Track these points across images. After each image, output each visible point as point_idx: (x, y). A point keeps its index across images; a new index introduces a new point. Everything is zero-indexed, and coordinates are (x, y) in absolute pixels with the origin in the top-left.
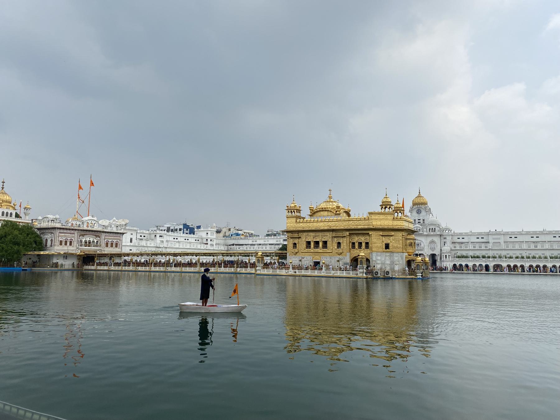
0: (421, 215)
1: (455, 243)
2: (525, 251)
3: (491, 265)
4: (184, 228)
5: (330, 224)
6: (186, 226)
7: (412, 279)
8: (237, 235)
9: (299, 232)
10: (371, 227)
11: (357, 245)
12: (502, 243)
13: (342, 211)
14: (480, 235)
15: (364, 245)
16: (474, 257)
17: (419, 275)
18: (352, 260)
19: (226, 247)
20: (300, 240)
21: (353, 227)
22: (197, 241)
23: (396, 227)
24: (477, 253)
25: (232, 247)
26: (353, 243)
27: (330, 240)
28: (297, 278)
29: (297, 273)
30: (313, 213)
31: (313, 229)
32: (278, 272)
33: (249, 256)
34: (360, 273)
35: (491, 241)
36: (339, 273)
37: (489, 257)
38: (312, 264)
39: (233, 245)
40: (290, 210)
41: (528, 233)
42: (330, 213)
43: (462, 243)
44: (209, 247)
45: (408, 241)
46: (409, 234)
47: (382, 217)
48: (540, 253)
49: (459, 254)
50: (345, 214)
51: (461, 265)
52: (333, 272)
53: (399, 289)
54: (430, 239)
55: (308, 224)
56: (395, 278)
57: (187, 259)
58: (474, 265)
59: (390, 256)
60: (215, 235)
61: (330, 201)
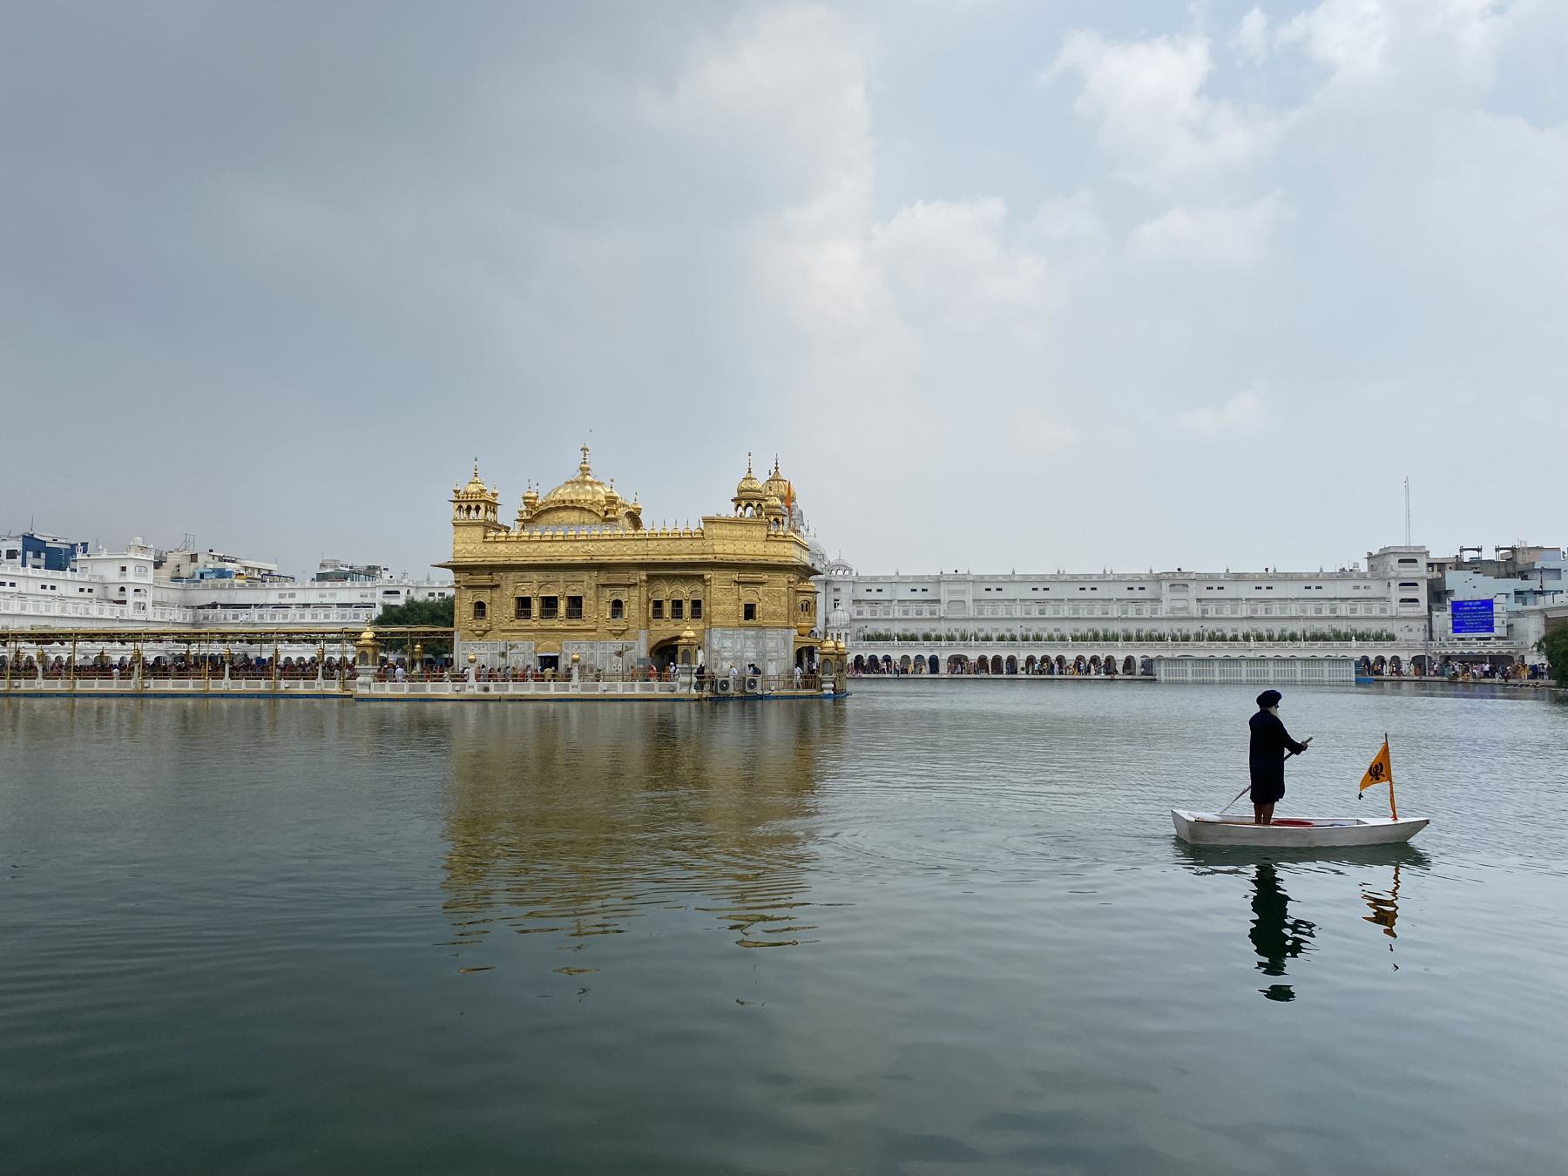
1: (859, 601)
2: (1019, 623)
3: (944, 657)
4: (26, 548)
5: (590, 547)
6: (32, 545)
7: (811, 697)
8: (222, 574)
9: (492, 569)
10: (710, 558)
11: (667, 609)
12: (970, 603)
13: (622, 512)
15: (687, 608)
16: (905, 638)
17: (828, 688)
18: (651, 652)
19: (190, 612)
21: (659, 559)
22: (86, 594)
23: (774, 561)
24: (912, 628)
25: (211, 612)
26: (658, 604)
27: (591, 593)
28: (491, 705)
30: (535, 514)
31: (540, 560)
32: (429, 689)
33: (314, 642)
34: (683, 684)
36: (620, 689)
37: (939, 638)
38: (535, 664)
39: (214, 606)
40: (466, 504)
41: (1025, 580)
42: (586, 517)
43: (877, 602)
44: (129, 612)
45: (802, 598)
46: (802, 580)
47: (738, 531)
48: (1049, 629)
49: (870, 629)
50: (627, 521)
51: (873, 659)
53: (775, 723)
55: (523, 547)
56: (768, 697)
57: (87, 652)
58: (906, 658)
59: (757, 638)
60: (150, 576)
61: (585, 482)
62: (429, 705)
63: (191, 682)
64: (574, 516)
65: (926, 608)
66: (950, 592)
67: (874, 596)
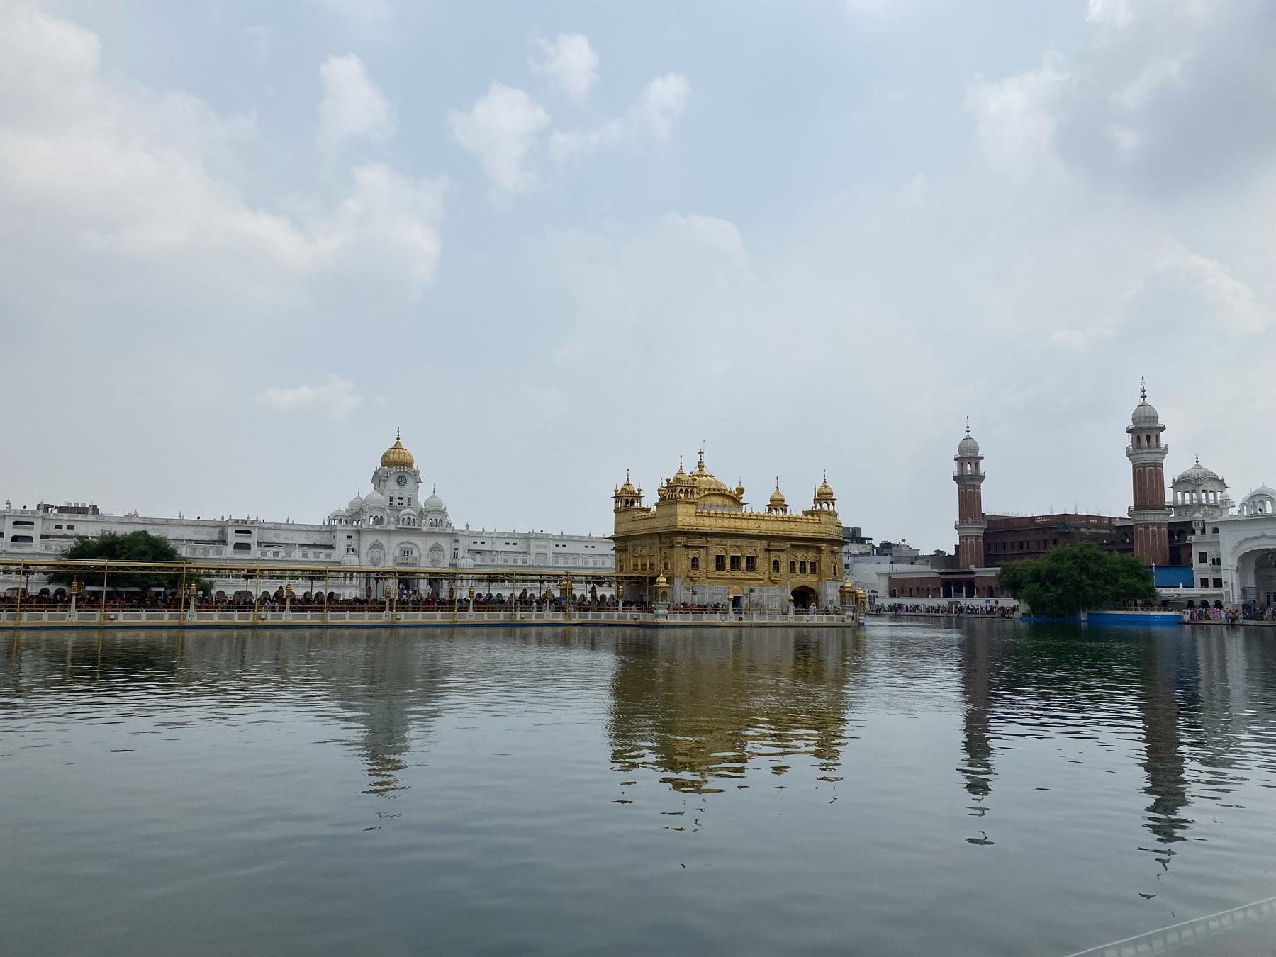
0: (406, 488)
5: (757, 523)
11: (798, 566)
12: (550, 556)
14: (512, 538)
15: (808, 566)
20: (703, 552)
21: (800, 535)
27: (761, 555)
28: (744, 630)
29: (744, 621)
35: (533, 550)
42: (727, 502)
43: (478, 552)
52: (805, 616)
54: (431, 542)
55: (719, 521)
62: (705, 631)
63: (439, 614)
64: (719, 500)
65: (520, 557)
66: (537, 547)
67: (478, 547)
